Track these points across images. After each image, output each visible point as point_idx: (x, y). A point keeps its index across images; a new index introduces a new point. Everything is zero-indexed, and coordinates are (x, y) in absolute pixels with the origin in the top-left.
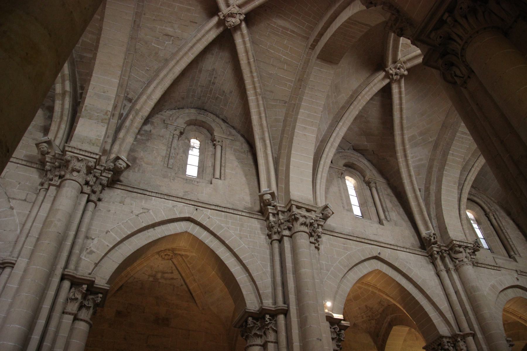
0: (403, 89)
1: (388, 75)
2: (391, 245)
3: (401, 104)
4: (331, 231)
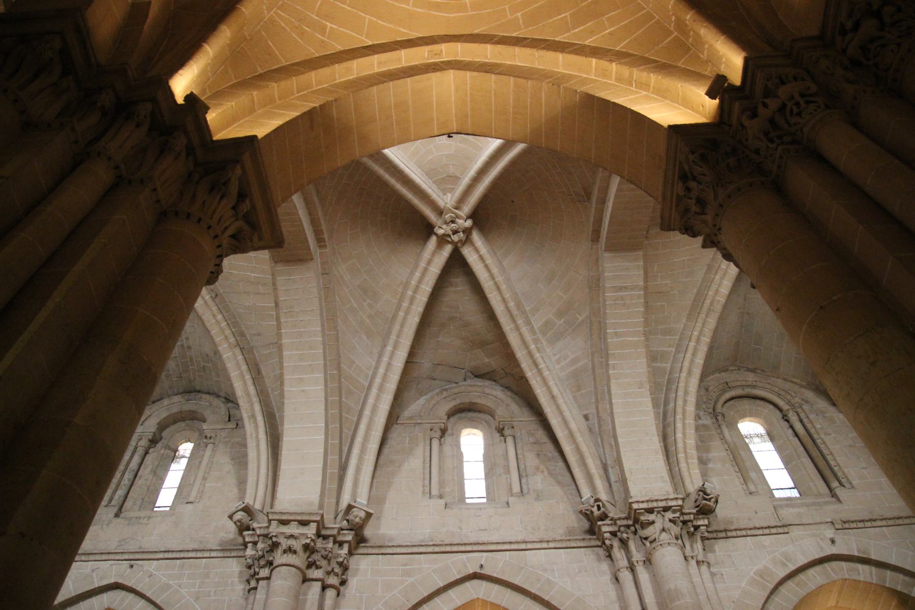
0: (483, 250)
4: (380, 547)
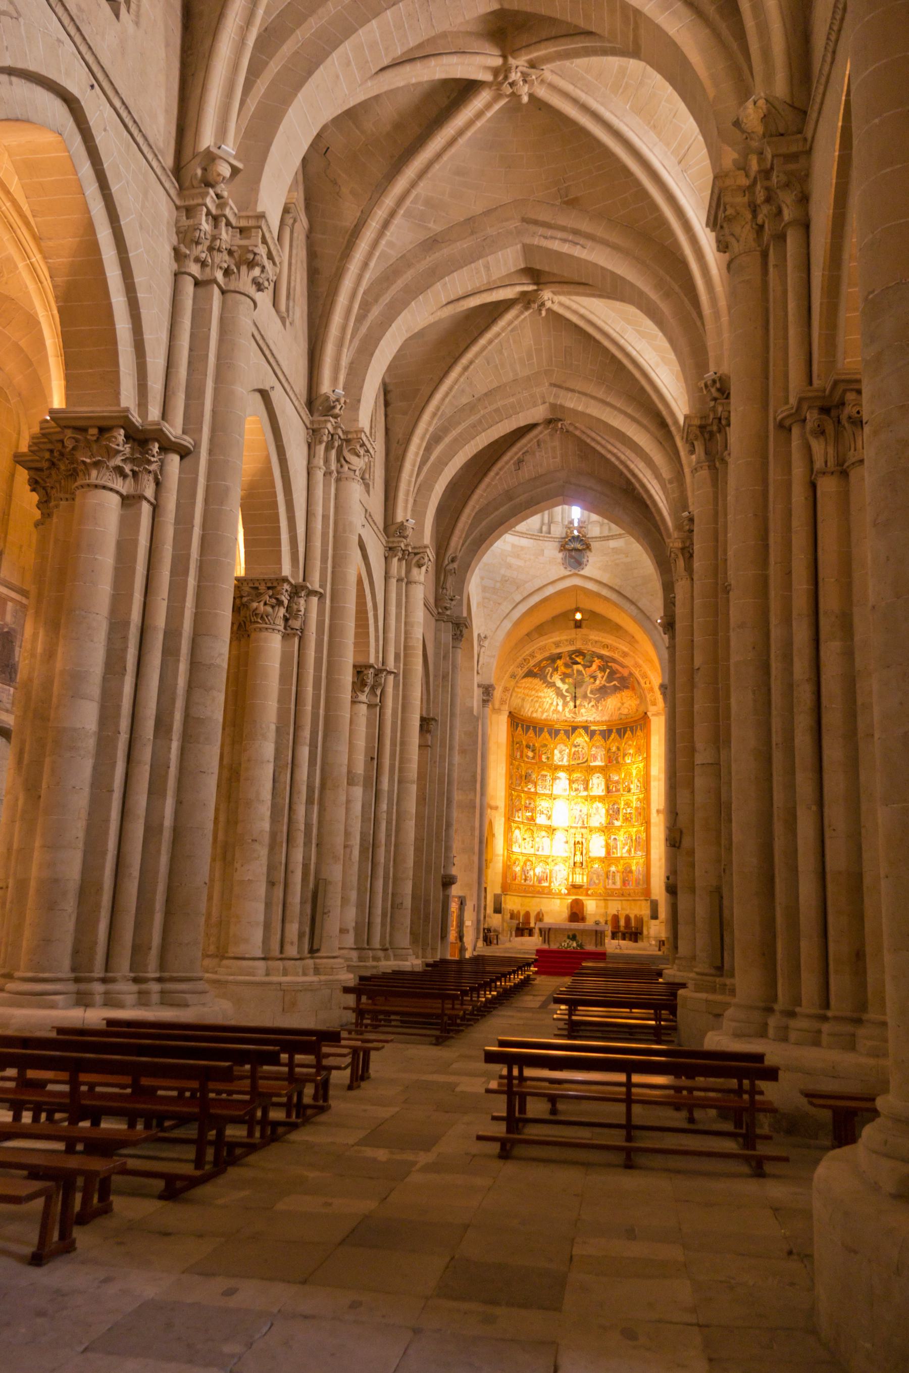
0: (489, 114)
1: (502, 72)
2: (287, 380)
3: (461, 133)
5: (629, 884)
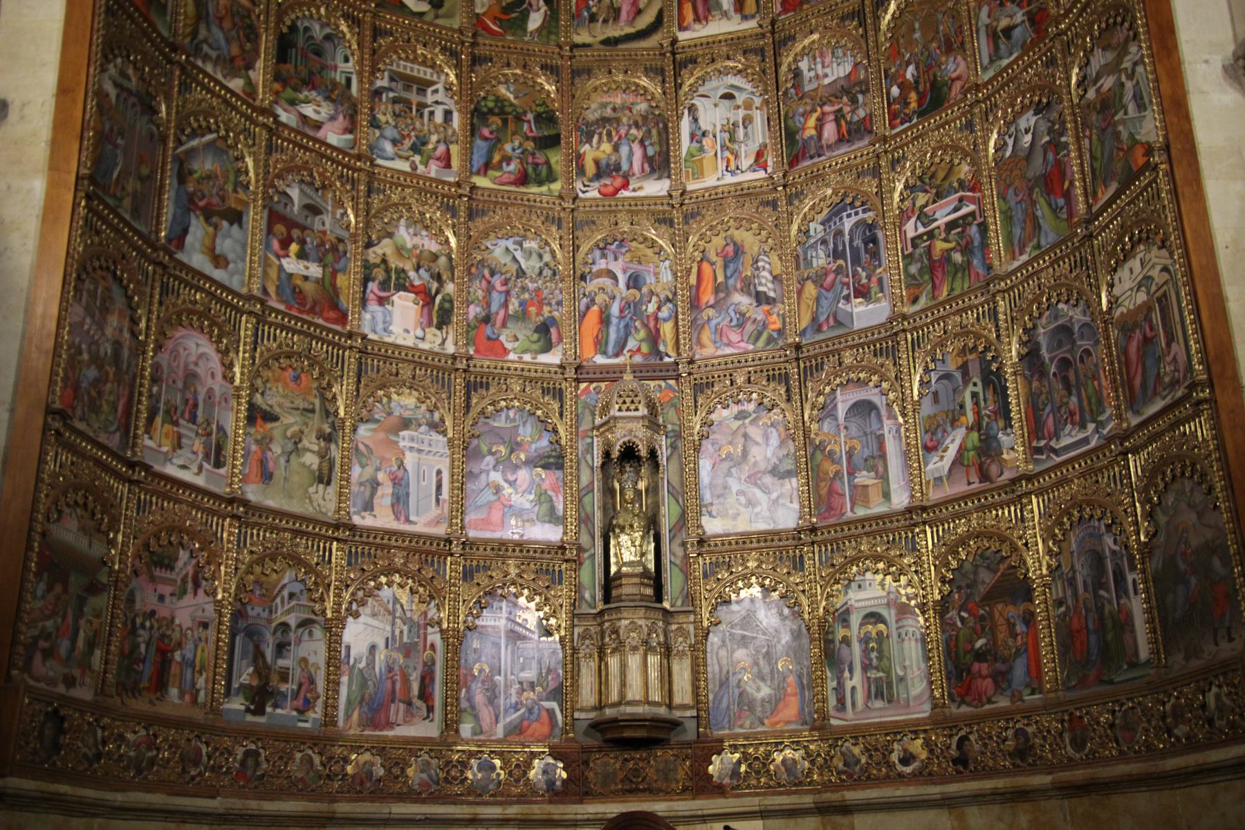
5: (1001, 679)
